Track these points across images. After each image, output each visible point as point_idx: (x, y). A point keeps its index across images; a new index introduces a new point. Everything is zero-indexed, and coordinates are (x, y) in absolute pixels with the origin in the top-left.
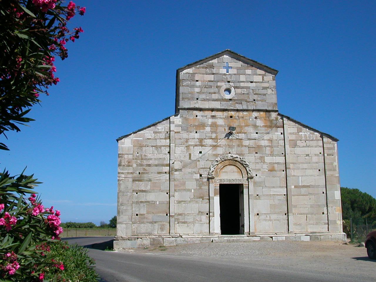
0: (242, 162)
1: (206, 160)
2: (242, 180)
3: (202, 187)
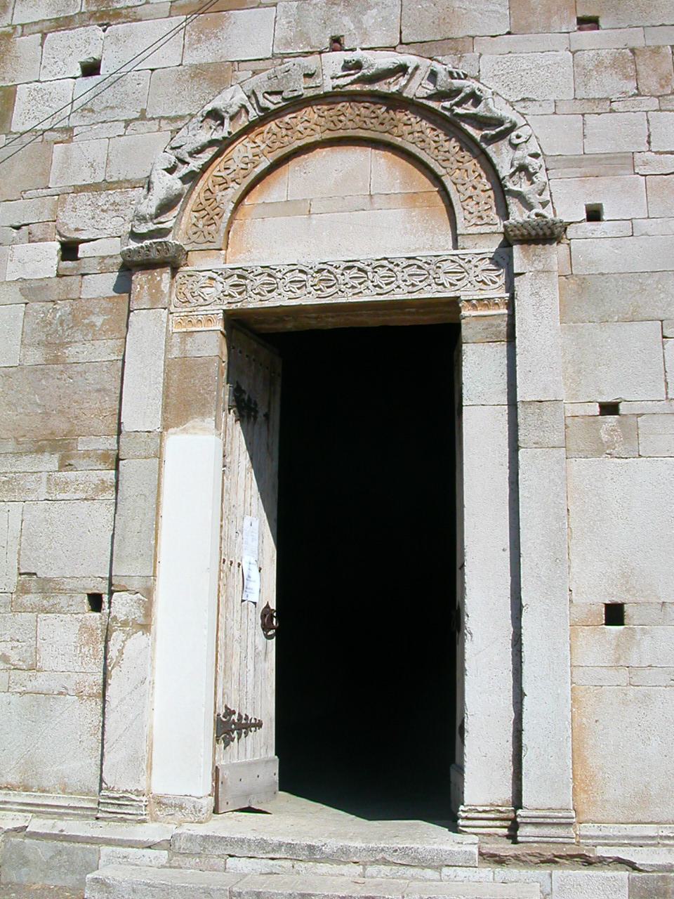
0: (447, 104)
1: (127, 123)
2: (447, 266)
3: (70, 351)
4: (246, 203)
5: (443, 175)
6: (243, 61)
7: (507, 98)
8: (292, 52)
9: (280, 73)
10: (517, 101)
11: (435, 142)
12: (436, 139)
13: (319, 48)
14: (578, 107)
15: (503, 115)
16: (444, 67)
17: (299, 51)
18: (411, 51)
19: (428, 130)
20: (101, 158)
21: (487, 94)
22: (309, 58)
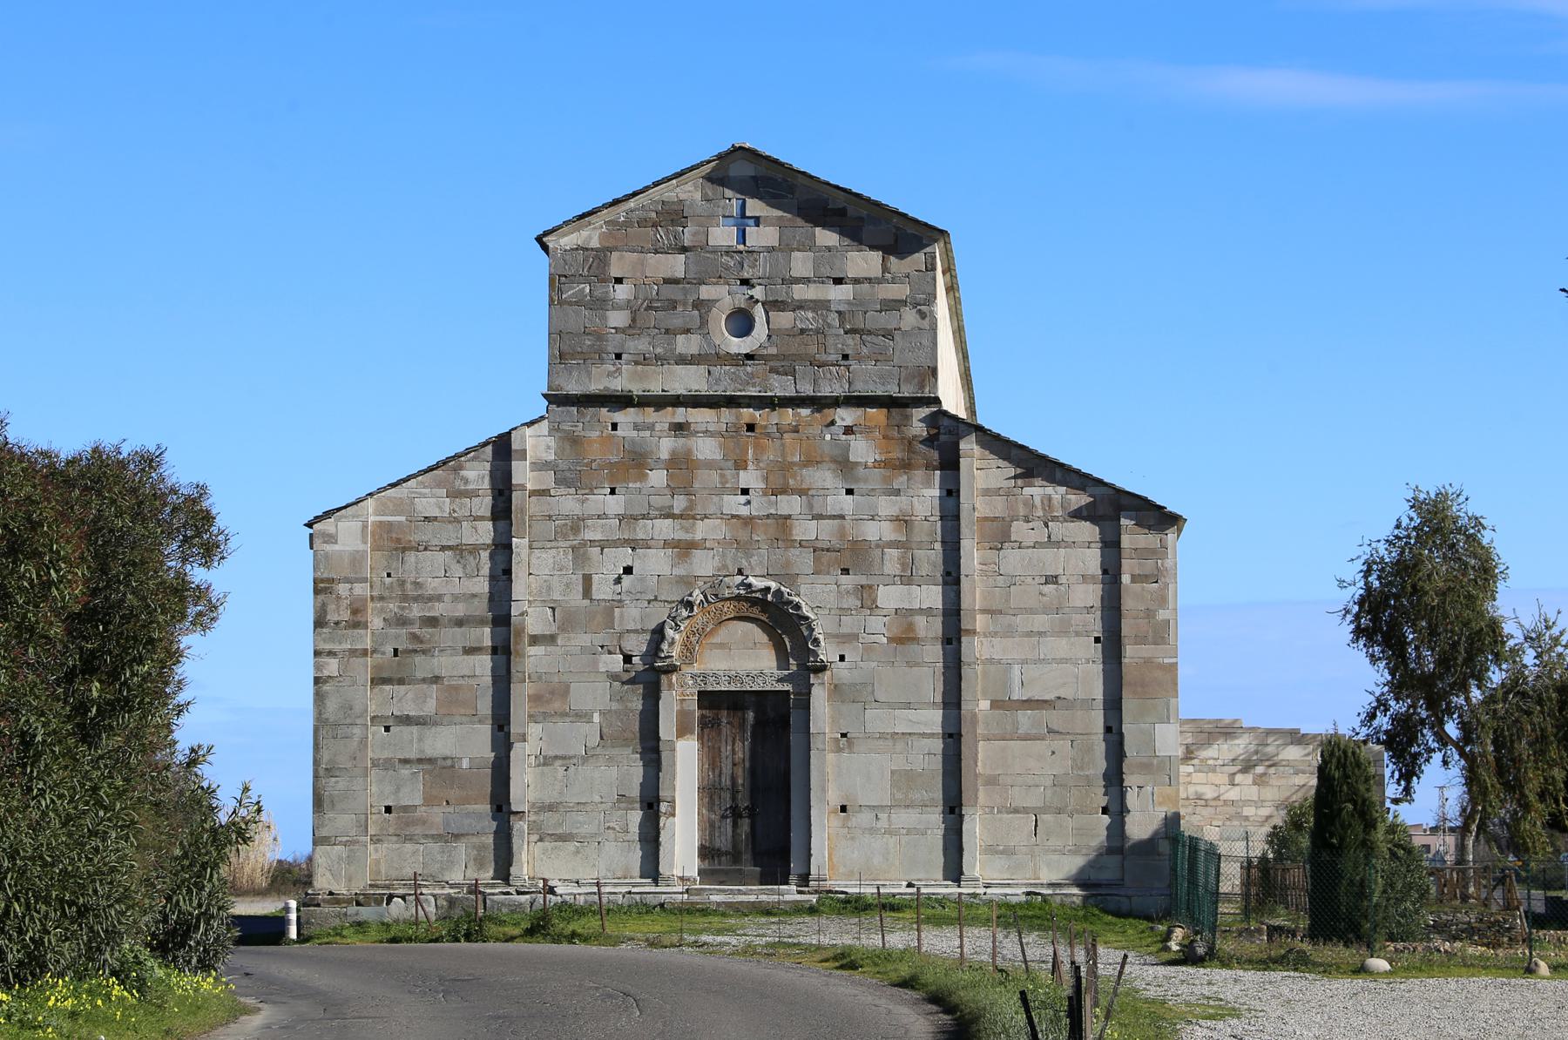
14: (838, 612)
20: (638, 617)
21: (803, 604)
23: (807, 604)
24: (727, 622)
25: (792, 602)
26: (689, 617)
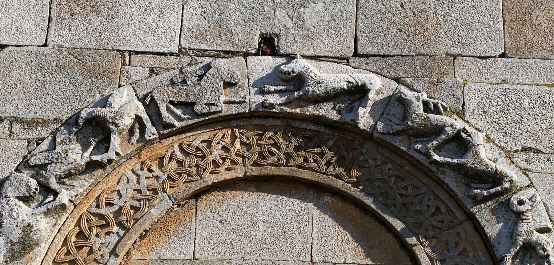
4: (134, 257)
5: (415, 245)
6: (137, 53)
7: (503, 145)
8: (208, 48)
9: (189, 76)
10: (516, 151)
11: (401, 195)
12: (404, 192)
13: (244, 47)
15: (499, 170)
16: (416, 94)
17: (215, 48)
18: (371, 68)
19: (393, 179)
21: (479, 138)
22: (231, 60)
23: (488, 139)
24: (218, 195)
25: (439, 129)
26: (92, 166)
